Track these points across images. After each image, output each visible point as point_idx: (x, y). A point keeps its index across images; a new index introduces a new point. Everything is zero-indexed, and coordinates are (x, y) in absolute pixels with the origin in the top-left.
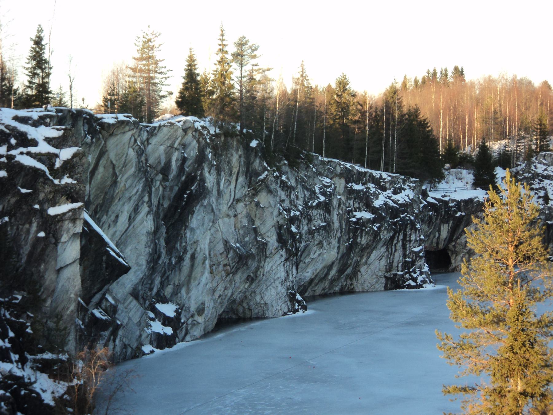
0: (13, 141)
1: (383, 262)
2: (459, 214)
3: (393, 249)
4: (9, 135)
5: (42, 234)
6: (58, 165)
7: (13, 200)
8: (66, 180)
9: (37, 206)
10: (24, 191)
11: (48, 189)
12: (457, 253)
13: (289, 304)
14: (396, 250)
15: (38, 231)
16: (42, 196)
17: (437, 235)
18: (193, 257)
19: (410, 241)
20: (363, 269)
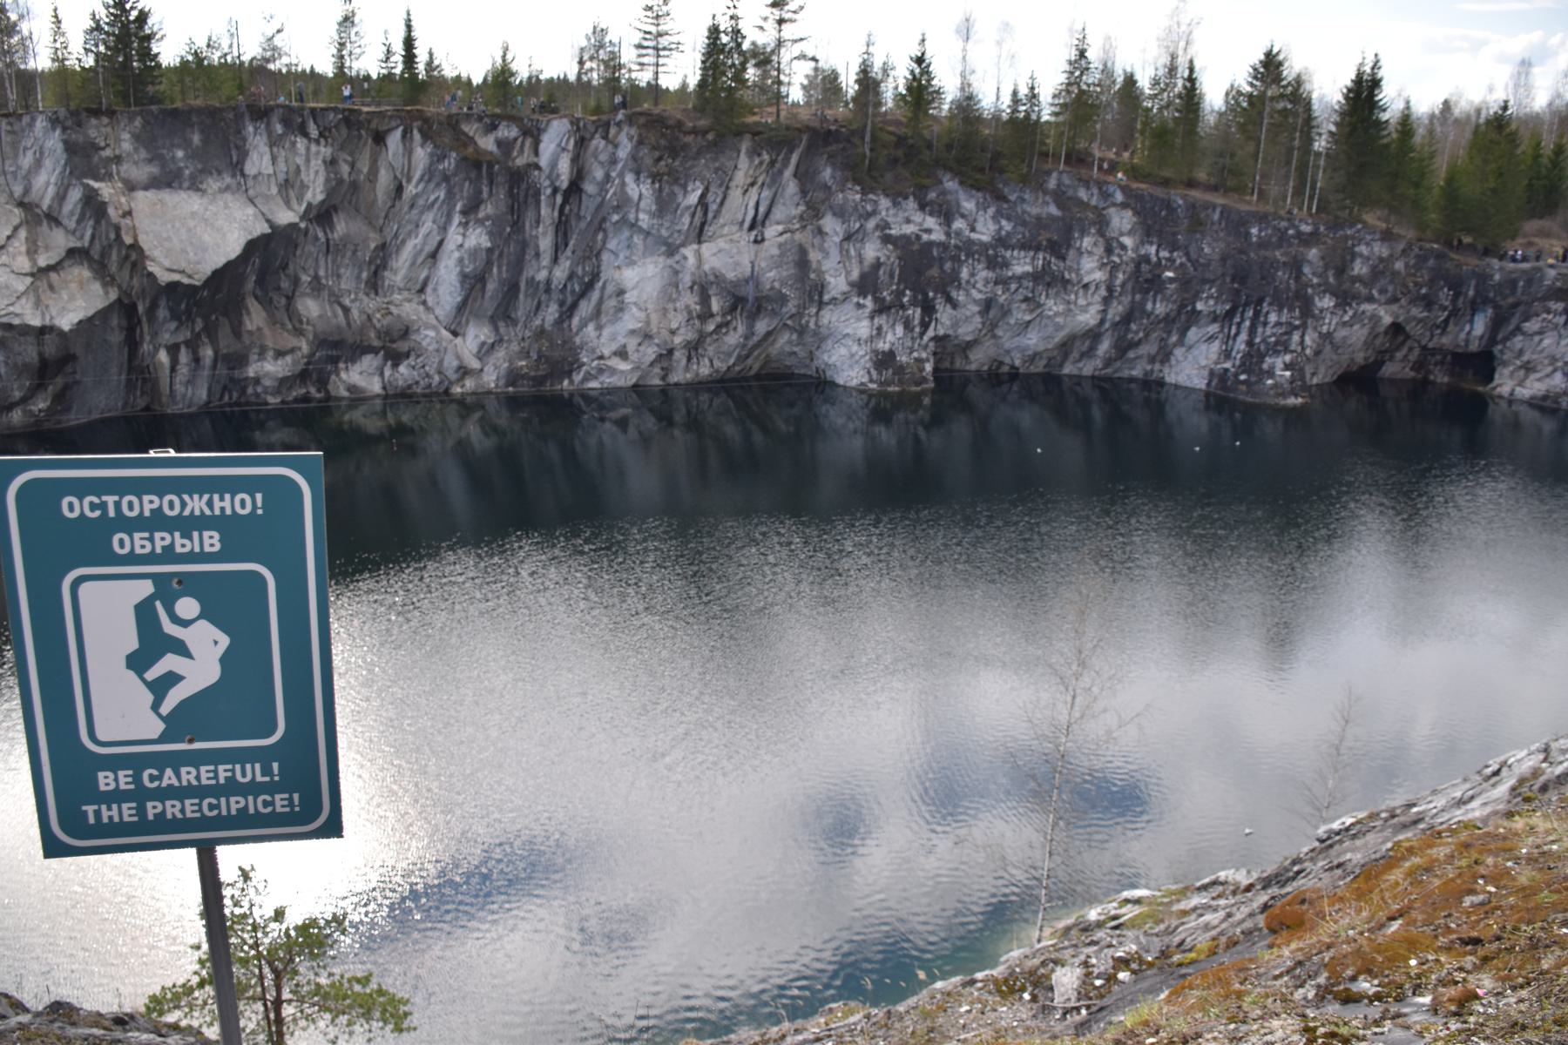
1: (1216, 346)
3: (1233, 331)
12: (1505, 364)
13: (874, 373)
14: (1237, 334)
17: (1467, 328)
18: (604, 287)
19: (1265, 324)
20: (1179, 352)
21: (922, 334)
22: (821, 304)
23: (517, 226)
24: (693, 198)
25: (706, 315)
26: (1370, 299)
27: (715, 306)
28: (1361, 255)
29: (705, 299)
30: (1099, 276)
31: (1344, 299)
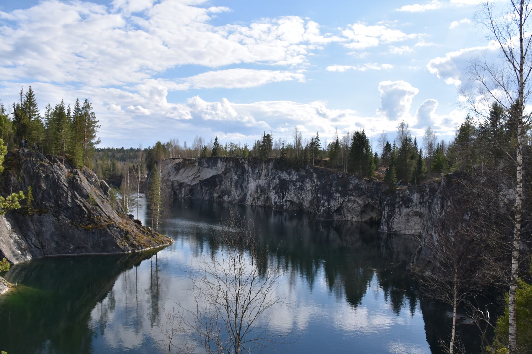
21: (283, 199)
22: (270, 192)
23: (243, 176)
24: (257, 171)
25: (258, 193)
26: (353, 195)
27: (259, 191)
28: (352, 183)
29: (257, 190)
30: (310, 188)
31: (344, 194)
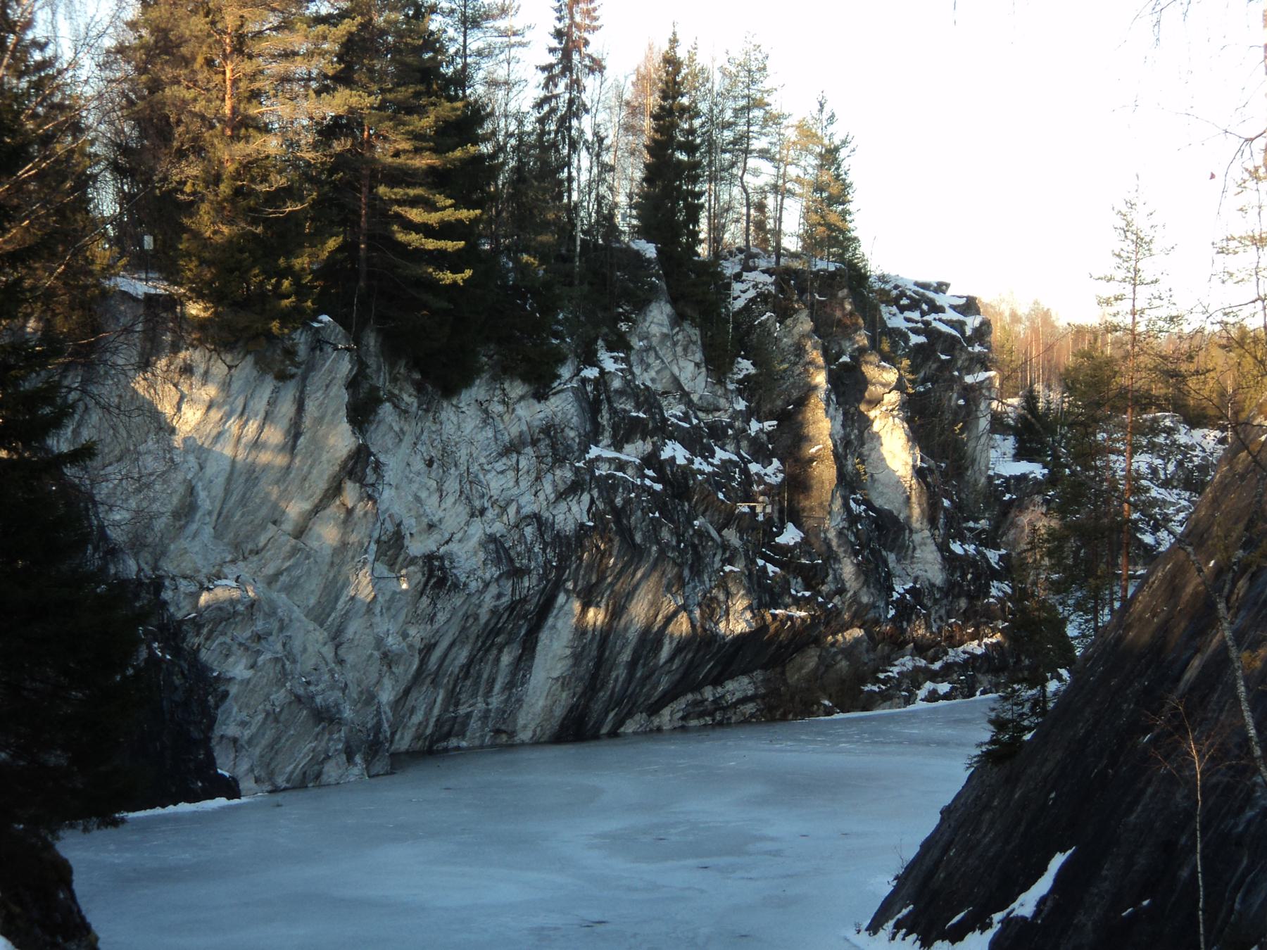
0: (925, 307)
2: (1007, 497)
4: (919, 301)
5: (961, 402)
6: (968, 332)
7: (934, 366)
8: (977, 349)
9: (956, 373)
10: (943, 357)
11: (964, 356)
15: (958, 399)
16: (960, 363)
